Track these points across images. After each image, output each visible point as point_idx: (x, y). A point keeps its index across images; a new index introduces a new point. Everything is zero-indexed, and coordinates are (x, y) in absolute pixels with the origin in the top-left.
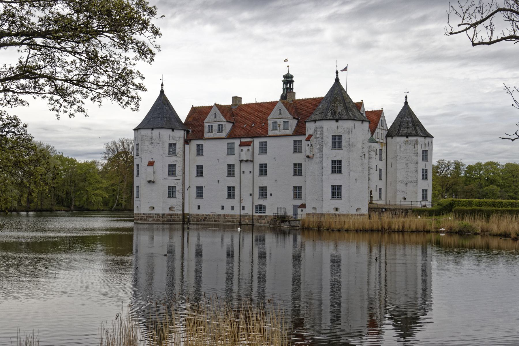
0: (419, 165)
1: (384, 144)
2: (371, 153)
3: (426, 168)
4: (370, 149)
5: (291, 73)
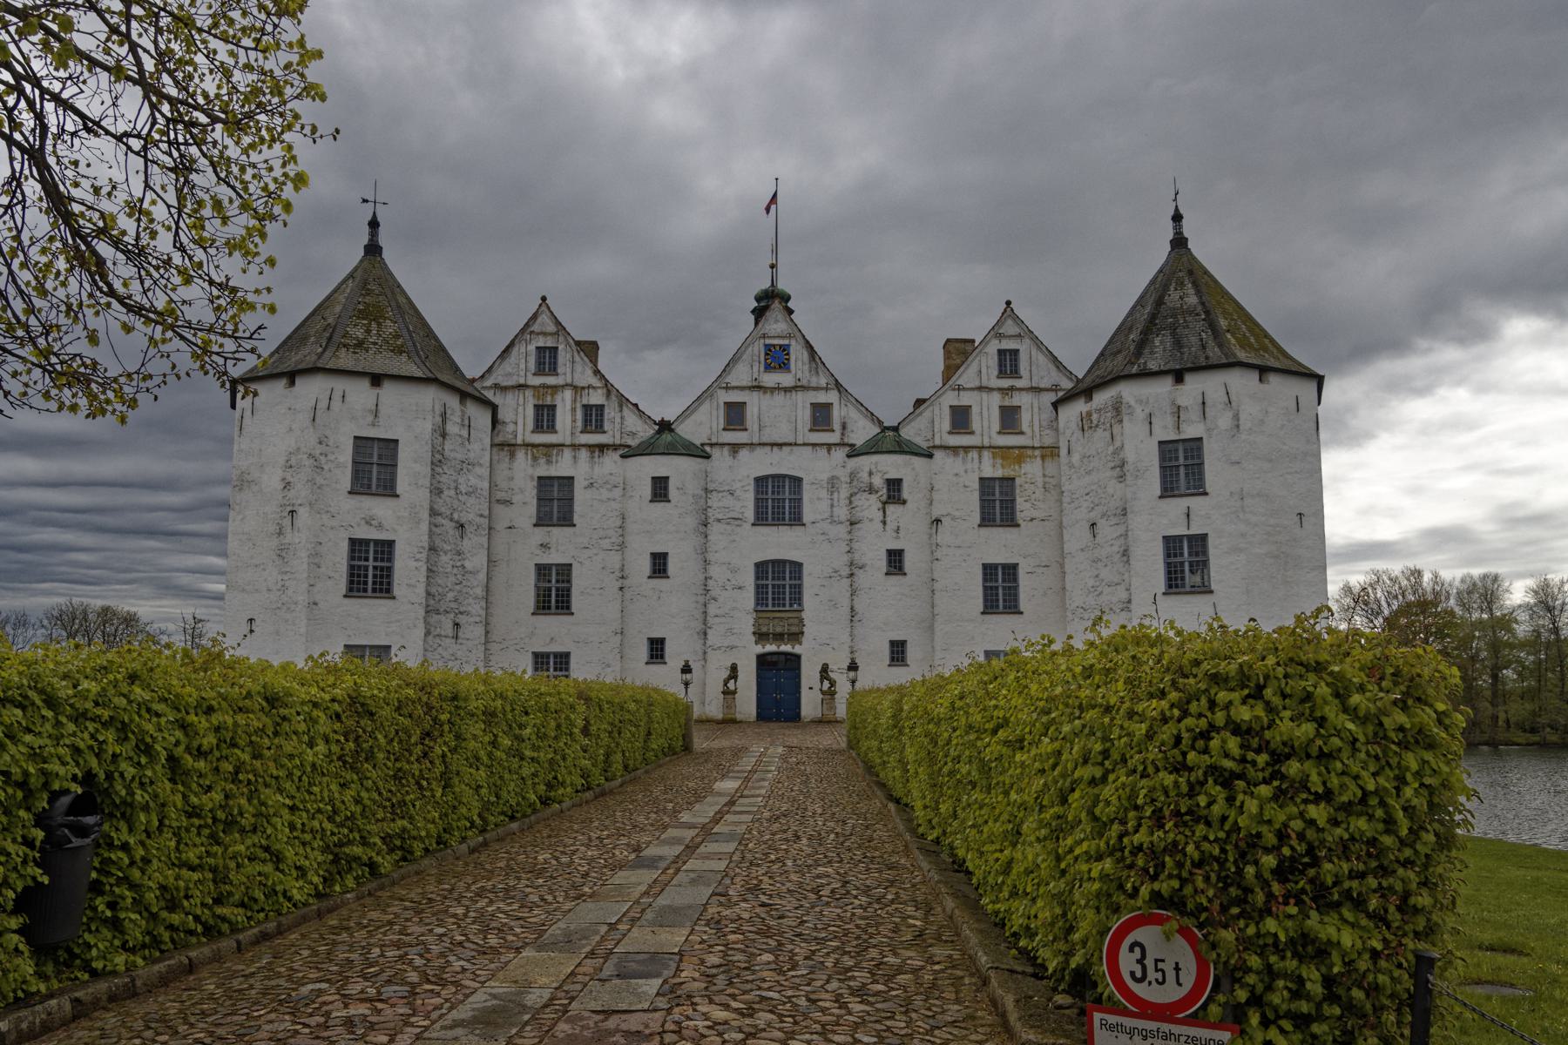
0: (1137, 522)
1: (1037, 453)
2: (857, 501)
3: (1195, 530)
4: (855, 483)
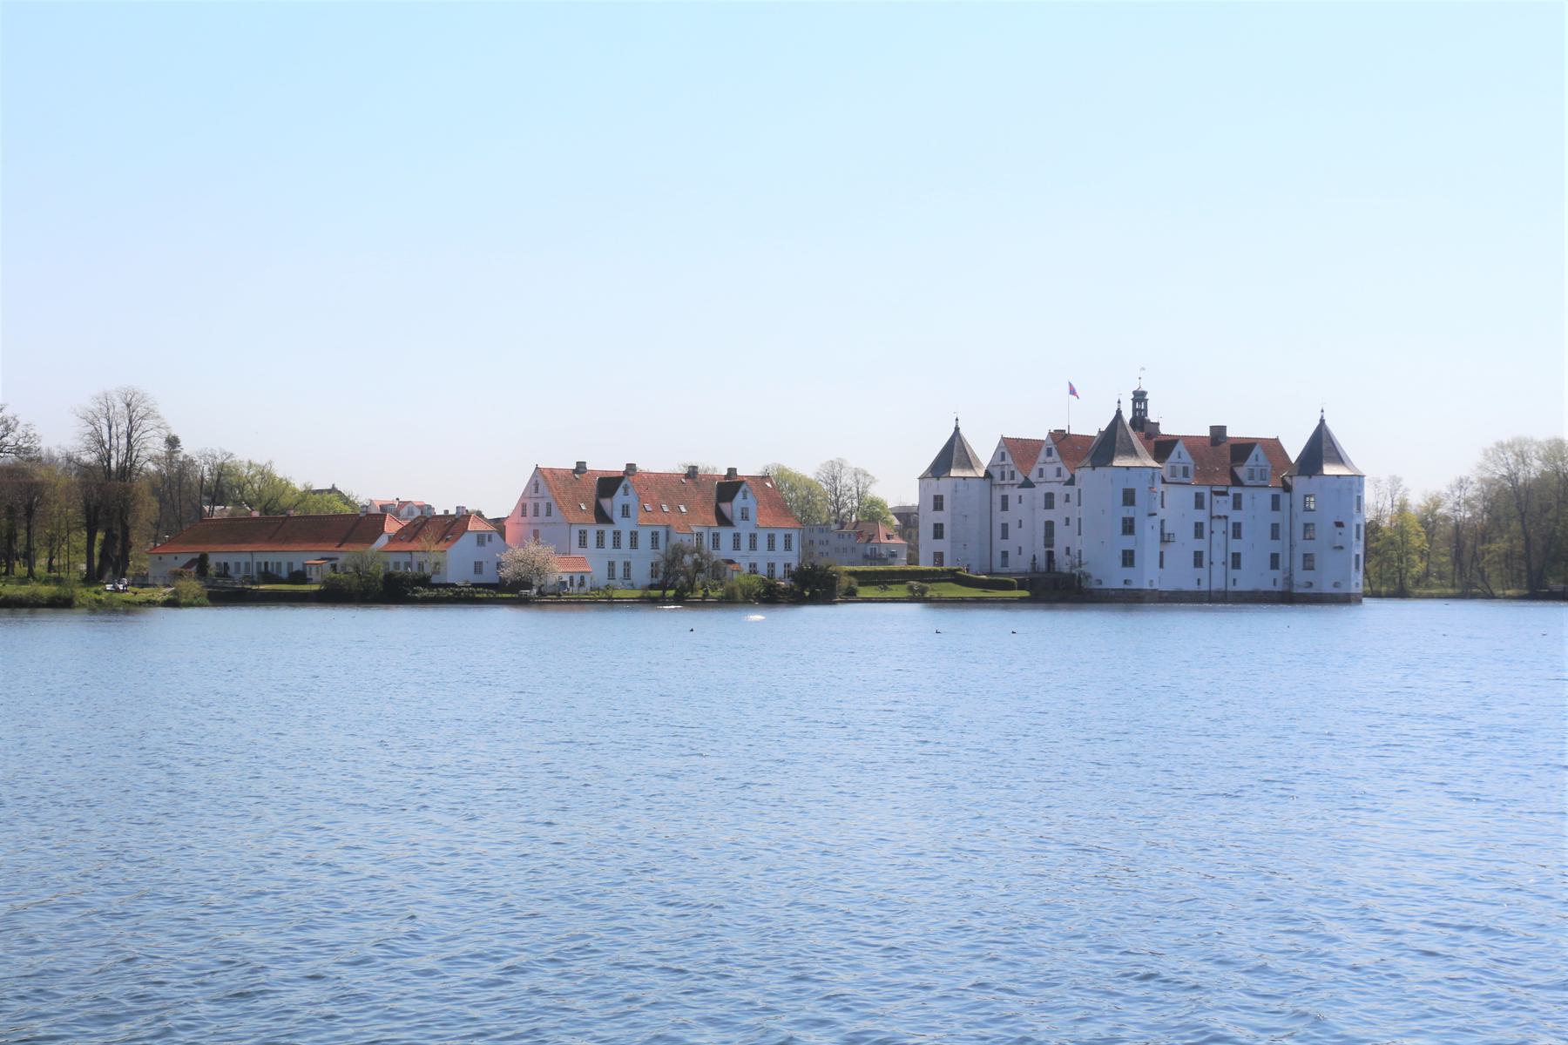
5: (1144, 388)
